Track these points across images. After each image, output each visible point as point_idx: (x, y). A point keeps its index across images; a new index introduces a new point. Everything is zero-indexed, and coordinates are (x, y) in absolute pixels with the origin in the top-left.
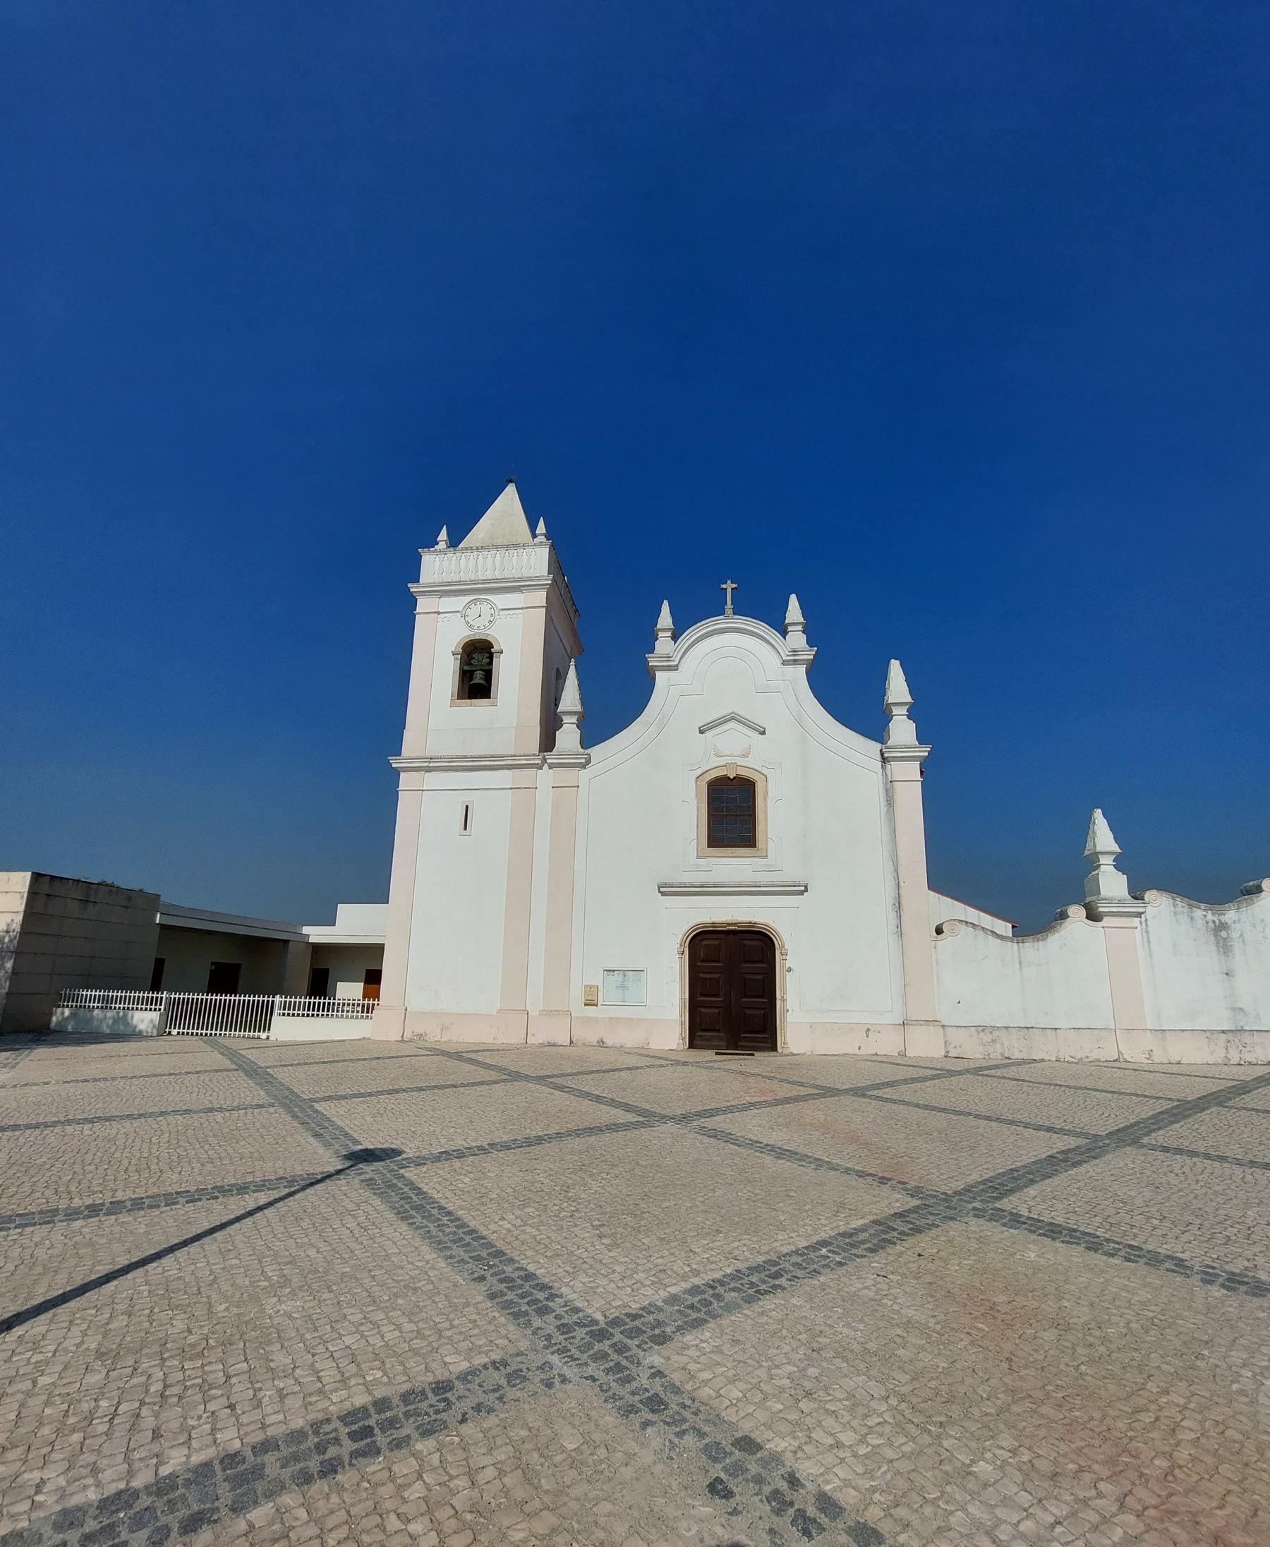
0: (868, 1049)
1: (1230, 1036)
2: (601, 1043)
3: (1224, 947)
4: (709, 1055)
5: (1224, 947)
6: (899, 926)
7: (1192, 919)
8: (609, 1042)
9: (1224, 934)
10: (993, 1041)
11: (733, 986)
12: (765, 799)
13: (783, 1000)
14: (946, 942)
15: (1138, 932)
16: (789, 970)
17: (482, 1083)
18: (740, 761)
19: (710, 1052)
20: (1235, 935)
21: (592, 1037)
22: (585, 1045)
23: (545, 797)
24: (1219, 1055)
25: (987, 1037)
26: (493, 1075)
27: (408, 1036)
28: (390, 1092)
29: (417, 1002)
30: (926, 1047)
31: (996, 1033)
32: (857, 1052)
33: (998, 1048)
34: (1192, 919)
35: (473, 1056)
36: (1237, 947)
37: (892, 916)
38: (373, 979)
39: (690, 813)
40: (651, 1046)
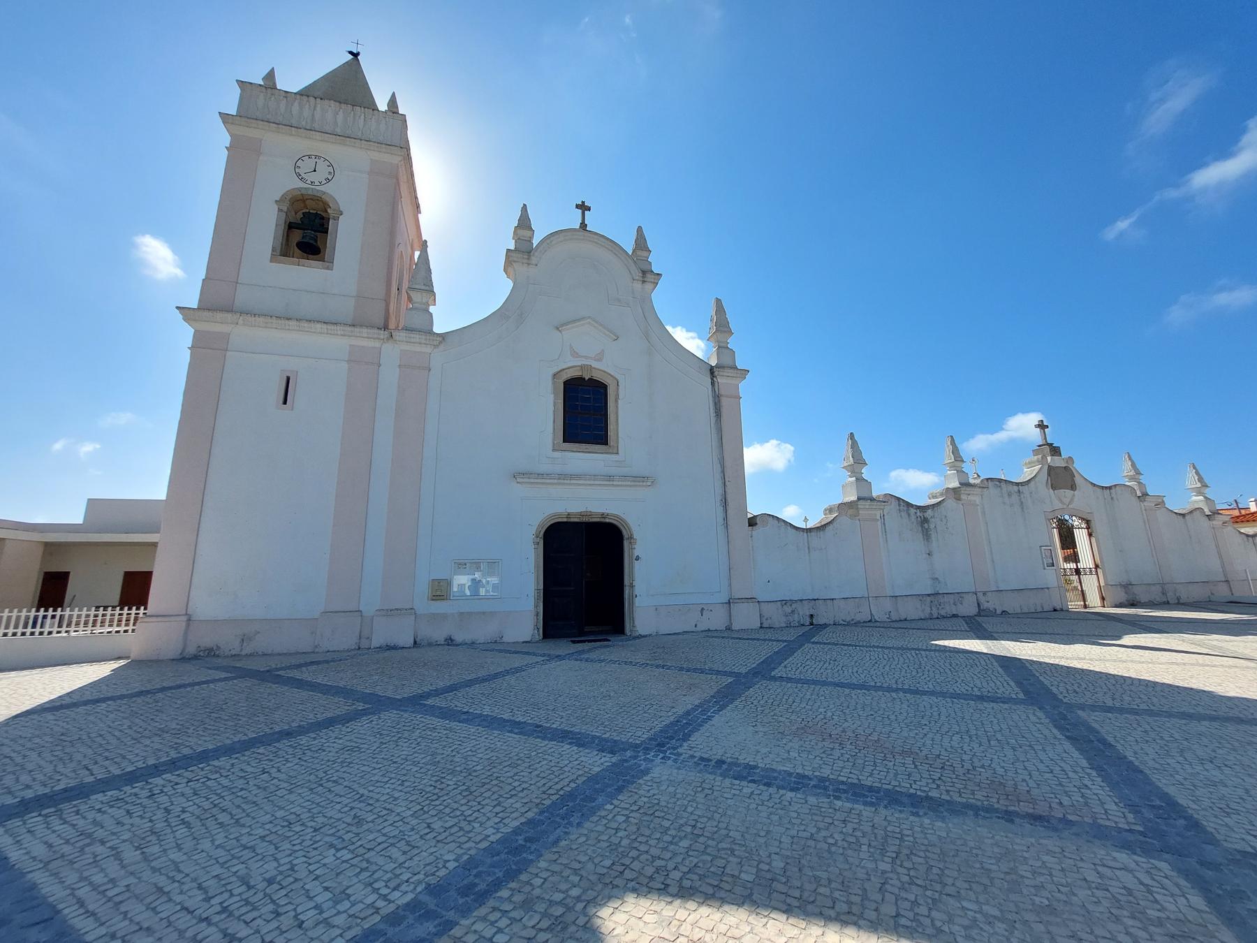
1: (932, 598)
2: (450, 641)
3: (926, 535)
4: (564, 647)
5: (926, 535)
6: (726, 519)
8: (459, 638)
10: (793, 612)
11: (584, 575)
12: (616, 401)
13: (632, 586)
14: (758, 531)
17: (330, 723)
18: (595, 364)
20: (932, 526)
21: (439, 635)
22: (430, 645)
23: (389, 375)
25: (788, 609)
27: (191, 650)
28: (173, 765)
29: (206, 606)
30: (746, 618)
32: (694, 629)
36: (933, 536)
38: (135, 589)
39: (546, 410)
40: (505, 640)
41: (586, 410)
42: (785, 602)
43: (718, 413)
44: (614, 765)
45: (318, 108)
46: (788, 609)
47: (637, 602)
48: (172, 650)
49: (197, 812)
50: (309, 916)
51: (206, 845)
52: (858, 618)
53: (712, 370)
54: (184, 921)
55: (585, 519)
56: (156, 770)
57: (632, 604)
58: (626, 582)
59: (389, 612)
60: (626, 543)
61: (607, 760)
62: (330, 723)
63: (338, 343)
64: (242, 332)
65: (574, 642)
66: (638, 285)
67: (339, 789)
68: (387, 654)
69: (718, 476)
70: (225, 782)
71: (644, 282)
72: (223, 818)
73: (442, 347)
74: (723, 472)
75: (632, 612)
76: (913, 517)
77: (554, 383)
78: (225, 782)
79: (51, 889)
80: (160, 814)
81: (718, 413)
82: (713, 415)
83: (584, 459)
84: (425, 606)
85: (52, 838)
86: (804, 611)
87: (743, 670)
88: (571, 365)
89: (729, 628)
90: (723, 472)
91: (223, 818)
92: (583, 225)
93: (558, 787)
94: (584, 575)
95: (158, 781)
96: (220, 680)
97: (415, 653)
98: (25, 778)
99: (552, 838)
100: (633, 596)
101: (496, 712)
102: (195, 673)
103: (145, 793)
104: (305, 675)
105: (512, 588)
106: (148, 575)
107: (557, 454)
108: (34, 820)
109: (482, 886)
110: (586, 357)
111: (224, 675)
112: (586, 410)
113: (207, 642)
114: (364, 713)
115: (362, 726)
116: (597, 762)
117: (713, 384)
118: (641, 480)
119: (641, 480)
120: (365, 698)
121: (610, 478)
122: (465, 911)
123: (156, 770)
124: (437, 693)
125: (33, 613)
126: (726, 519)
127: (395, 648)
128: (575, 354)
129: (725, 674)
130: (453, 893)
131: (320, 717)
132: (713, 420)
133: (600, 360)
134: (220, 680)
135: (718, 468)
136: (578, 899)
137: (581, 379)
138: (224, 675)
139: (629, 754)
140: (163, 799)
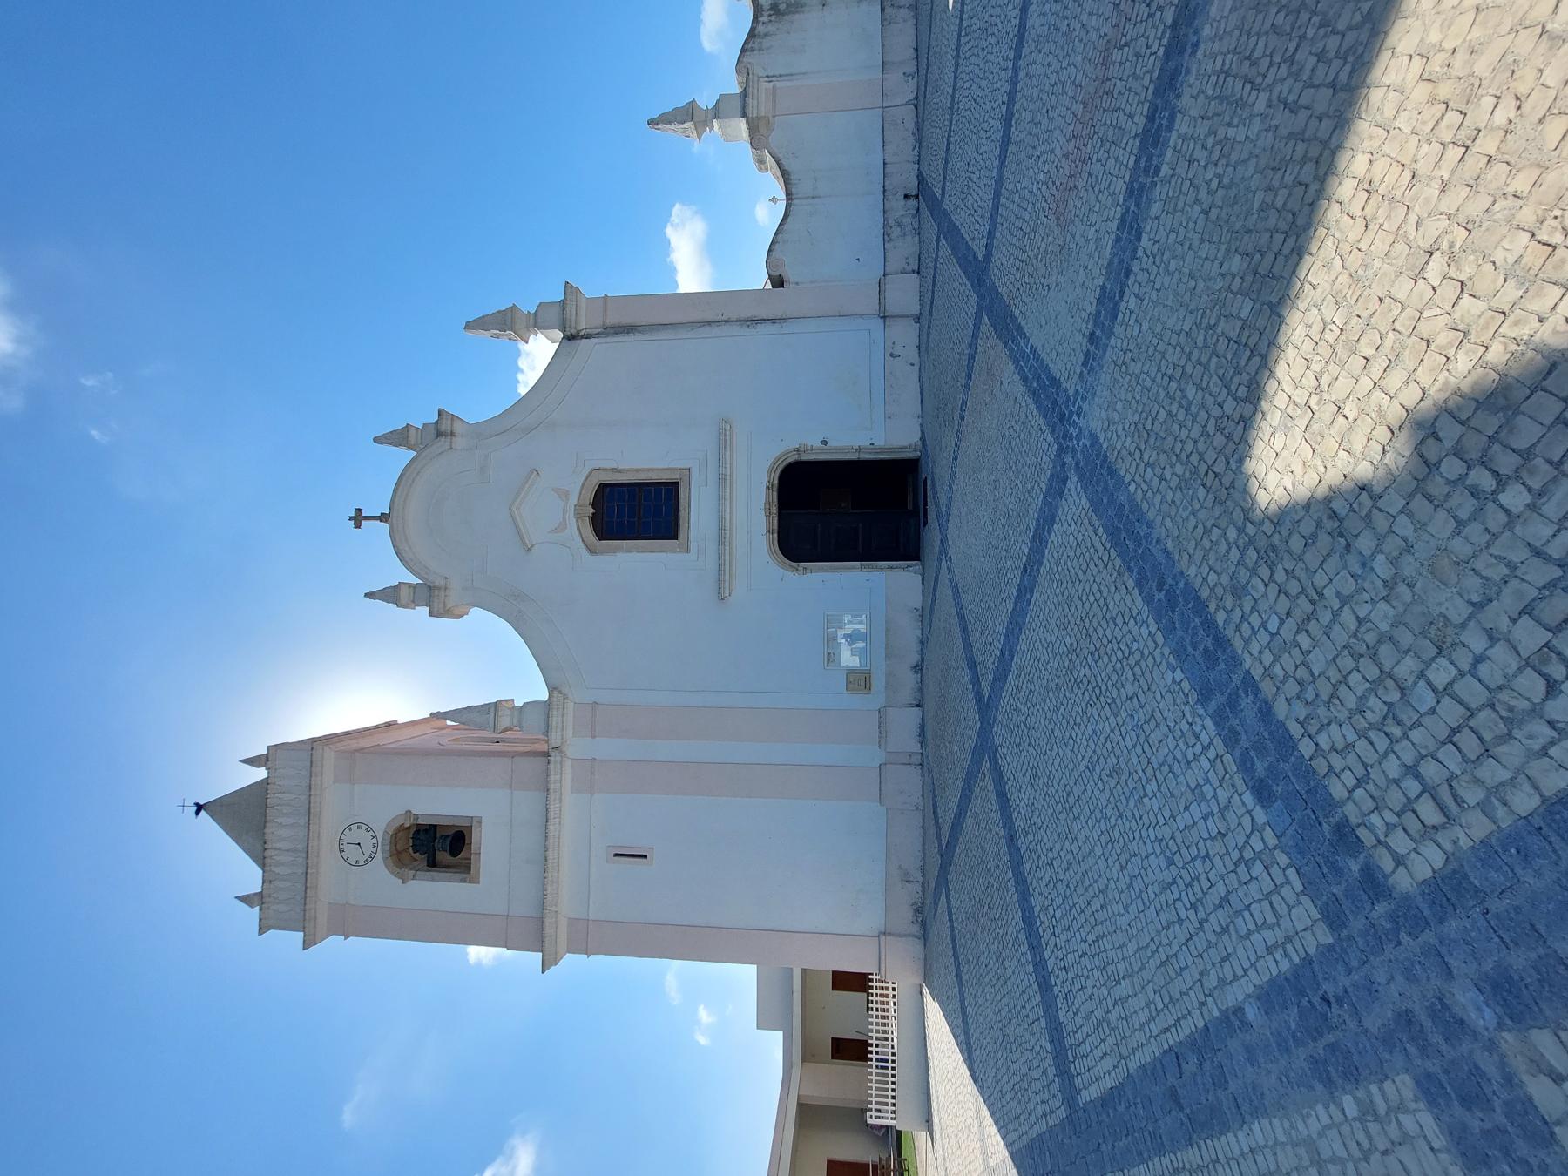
0: (913, 355)
2: (918, 668)
6: (773, 321)
7: (766, 35)
8: (915, 658)
9: (782, 7)
10: (899, 225)
11: (844, 509)
12: (620, 471)
13: (859, 450)
14: (790, 274)
15: (778, 85)
16: (824, 442)
17: (1002, 796)
18: (574, 500)
19: (923, 534)
21: (910, 679)
22: (921, 690)
24: (904, 12)
25: (896, 232)
26: (986, 784)
27: (916, 929)
28: (1035, 948)
29: (871, 918)
30: (905, 294)
31: (891, 222)
32: (917, 367)
33: (906, 220)
34: (766, 35)
35: (946, 829)
37: (761, 328)
39: (635, 560)
40: (919, 606)
41: (635, 511)
42: (886, 237)
43: (629, 329)
44: (1081, 479)
45: (278, 845)
46: (896, 232)
47: (879, 443)
48: (916, 947)
49: (1087, 928)
50: (1214, 826)
51: (1122, 922)
52: (911, 126)
53: (570, 338)
54: (1199, 943)
55: (775, 510)
56: (1040, 964)
57: (882, 450)
58: (854, 457)
59: (883, 736)
60: (805, 458)
61: (1074, 485)
62: (1002, 796)
63: (570, 807)
64: (566, 904)
65: (926, 523)
66: (459, 442)
67: (1077, 791)
68: (929, 735)
69: (715, 330)
70: (1058, 901)
71: (452, 434)
72: (1096, 904)
73: (565, 690)
74: (709, 323)
75: (891, 450)
76: (770, 28)
77: (602, 553)
78: (1058, 901)
79: (1147, 1055)
80: (1085, 962)
81: (629, 329)
82: (632, 337)
83: (698, 511)
84: (877, 698)
85: (1098, 1053)
86: (900, 208)
87: (974, 299)
88: (577, 531)
89: (917, 319)
90: (709, 323)
91: (1096, 904)
92: (383, 518)
93: (1100, 549)
94: (844, 509)
95: (1051, 963)
96: (948, 902)
97: (930, 704)
98: (1036, 1074)
99: (1161, 558)
100: (873, 448)
101: (1004, 617)
102: (940, 927)
103: (1063, 974)
104: (947, 819)
105: (857, 602)
106: (834, 973)
107: (693, 546)
108: (1077, 1067)
109: (1209, 642)
110: (565, 511)
111: (943, 899)
112: (635, 511)
113: (908, 914)
114: (994, 761)
115: (1008, 764)
116: (1076, 500)
117: (588, 336)
118: (723, 439)
119: (723, 439)
120: (976, 762)
121: (721, 479)
122: (1235, 662)
123: (1040, 964)
124: (976, 682)
125: (874, 1063)
126: (773, 321)
127: (922, 728)
128: (561, 527)
129: (977, 326)
130: (1212, 675)
131: (996, 806)
132: (638, 337)
133: (567, 494)
134: (948, 902)
135: (706, 330)
136: (1241, 530)
137: (594, 518)
138: (943, 899)
139: (1068, 460)
140: (1070, 959)
